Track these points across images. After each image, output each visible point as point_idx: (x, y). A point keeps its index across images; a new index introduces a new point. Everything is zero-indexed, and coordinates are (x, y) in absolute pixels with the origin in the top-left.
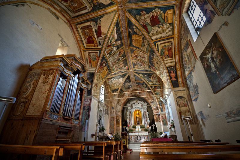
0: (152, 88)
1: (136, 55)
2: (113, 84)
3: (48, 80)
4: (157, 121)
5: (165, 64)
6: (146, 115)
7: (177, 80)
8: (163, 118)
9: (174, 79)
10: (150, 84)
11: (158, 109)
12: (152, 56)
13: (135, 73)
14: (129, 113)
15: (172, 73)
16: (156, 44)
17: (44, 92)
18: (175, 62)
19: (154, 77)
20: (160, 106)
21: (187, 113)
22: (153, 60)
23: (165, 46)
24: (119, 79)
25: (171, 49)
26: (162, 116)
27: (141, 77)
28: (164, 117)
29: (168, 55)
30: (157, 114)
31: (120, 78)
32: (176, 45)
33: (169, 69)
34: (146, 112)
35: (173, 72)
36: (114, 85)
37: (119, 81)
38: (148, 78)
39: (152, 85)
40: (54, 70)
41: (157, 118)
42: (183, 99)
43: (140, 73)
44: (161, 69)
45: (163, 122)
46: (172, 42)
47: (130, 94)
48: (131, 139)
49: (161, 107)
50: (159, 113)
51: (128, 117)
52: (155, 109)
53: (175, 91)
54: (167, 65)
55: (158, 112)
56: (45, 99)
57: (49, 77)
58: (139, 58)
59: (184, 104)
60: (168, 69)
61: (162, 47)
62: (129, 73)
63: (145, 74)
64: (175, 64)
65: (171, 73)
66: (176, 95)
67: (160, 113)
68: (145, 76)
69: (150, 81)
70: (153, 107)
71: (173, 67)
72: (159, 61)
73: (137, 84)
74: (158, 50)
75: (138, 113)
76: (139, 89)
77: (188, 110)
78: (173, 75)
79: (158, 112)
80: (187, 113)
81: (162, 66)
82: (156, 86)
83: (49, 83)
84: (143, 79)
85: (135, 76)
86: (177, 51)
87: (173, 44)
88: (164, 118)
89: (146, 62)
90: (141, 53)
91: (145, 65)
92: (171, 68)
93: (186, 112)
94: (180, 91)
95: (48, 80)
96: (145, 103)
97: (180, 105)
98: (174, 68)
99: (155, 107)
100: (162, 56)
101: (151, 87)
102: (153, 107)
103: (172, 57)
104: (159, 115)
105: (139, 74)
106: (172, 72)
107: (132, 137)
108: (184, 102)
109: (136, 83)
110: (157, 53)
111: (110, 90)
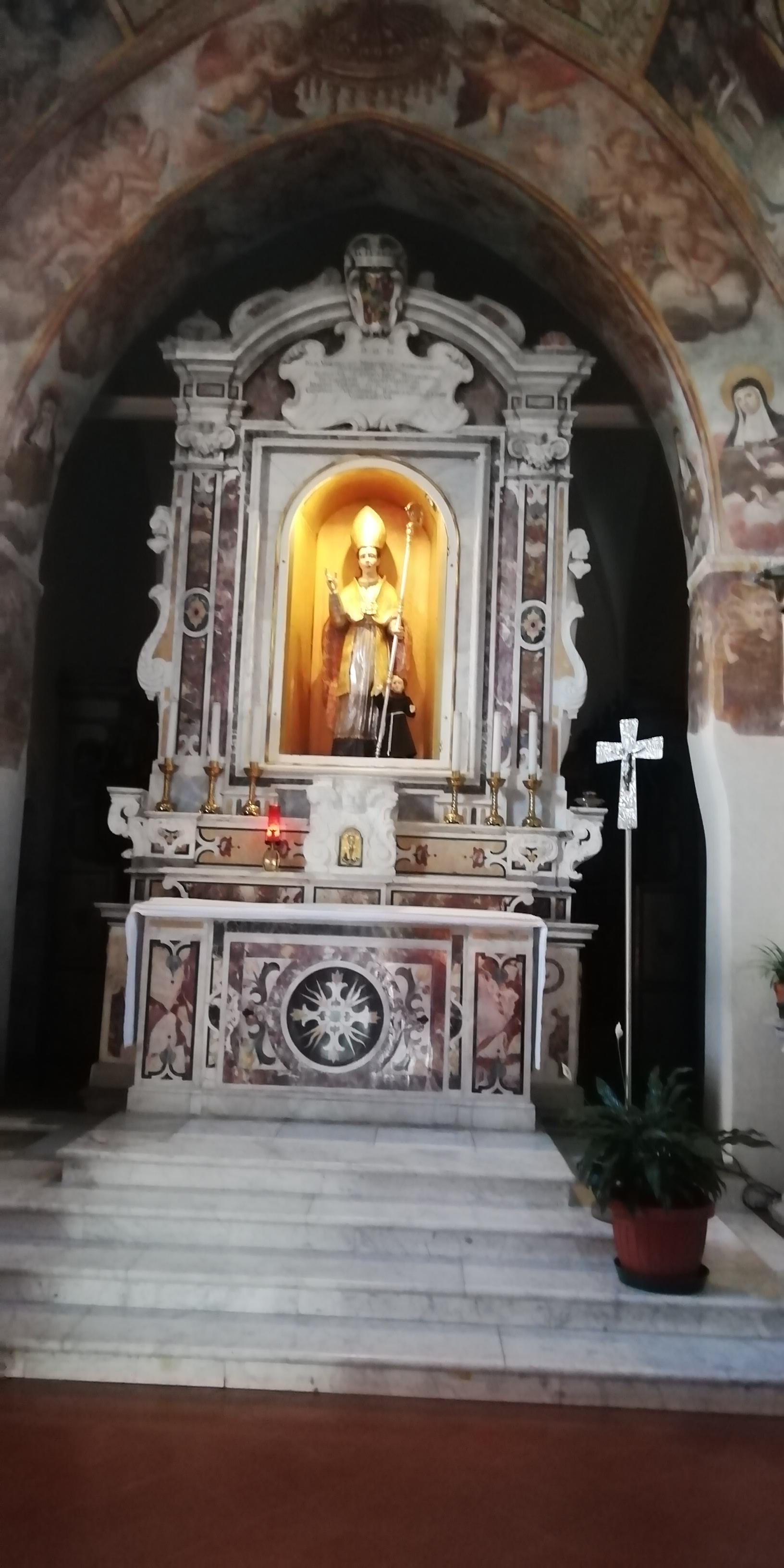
14: (198, 523)
34: (537, 534)
47: (241, 102)
48: (167, 1024)
51: (160, 594)
75: (382, 552)
96: (555, 342)
107: (188, 993)
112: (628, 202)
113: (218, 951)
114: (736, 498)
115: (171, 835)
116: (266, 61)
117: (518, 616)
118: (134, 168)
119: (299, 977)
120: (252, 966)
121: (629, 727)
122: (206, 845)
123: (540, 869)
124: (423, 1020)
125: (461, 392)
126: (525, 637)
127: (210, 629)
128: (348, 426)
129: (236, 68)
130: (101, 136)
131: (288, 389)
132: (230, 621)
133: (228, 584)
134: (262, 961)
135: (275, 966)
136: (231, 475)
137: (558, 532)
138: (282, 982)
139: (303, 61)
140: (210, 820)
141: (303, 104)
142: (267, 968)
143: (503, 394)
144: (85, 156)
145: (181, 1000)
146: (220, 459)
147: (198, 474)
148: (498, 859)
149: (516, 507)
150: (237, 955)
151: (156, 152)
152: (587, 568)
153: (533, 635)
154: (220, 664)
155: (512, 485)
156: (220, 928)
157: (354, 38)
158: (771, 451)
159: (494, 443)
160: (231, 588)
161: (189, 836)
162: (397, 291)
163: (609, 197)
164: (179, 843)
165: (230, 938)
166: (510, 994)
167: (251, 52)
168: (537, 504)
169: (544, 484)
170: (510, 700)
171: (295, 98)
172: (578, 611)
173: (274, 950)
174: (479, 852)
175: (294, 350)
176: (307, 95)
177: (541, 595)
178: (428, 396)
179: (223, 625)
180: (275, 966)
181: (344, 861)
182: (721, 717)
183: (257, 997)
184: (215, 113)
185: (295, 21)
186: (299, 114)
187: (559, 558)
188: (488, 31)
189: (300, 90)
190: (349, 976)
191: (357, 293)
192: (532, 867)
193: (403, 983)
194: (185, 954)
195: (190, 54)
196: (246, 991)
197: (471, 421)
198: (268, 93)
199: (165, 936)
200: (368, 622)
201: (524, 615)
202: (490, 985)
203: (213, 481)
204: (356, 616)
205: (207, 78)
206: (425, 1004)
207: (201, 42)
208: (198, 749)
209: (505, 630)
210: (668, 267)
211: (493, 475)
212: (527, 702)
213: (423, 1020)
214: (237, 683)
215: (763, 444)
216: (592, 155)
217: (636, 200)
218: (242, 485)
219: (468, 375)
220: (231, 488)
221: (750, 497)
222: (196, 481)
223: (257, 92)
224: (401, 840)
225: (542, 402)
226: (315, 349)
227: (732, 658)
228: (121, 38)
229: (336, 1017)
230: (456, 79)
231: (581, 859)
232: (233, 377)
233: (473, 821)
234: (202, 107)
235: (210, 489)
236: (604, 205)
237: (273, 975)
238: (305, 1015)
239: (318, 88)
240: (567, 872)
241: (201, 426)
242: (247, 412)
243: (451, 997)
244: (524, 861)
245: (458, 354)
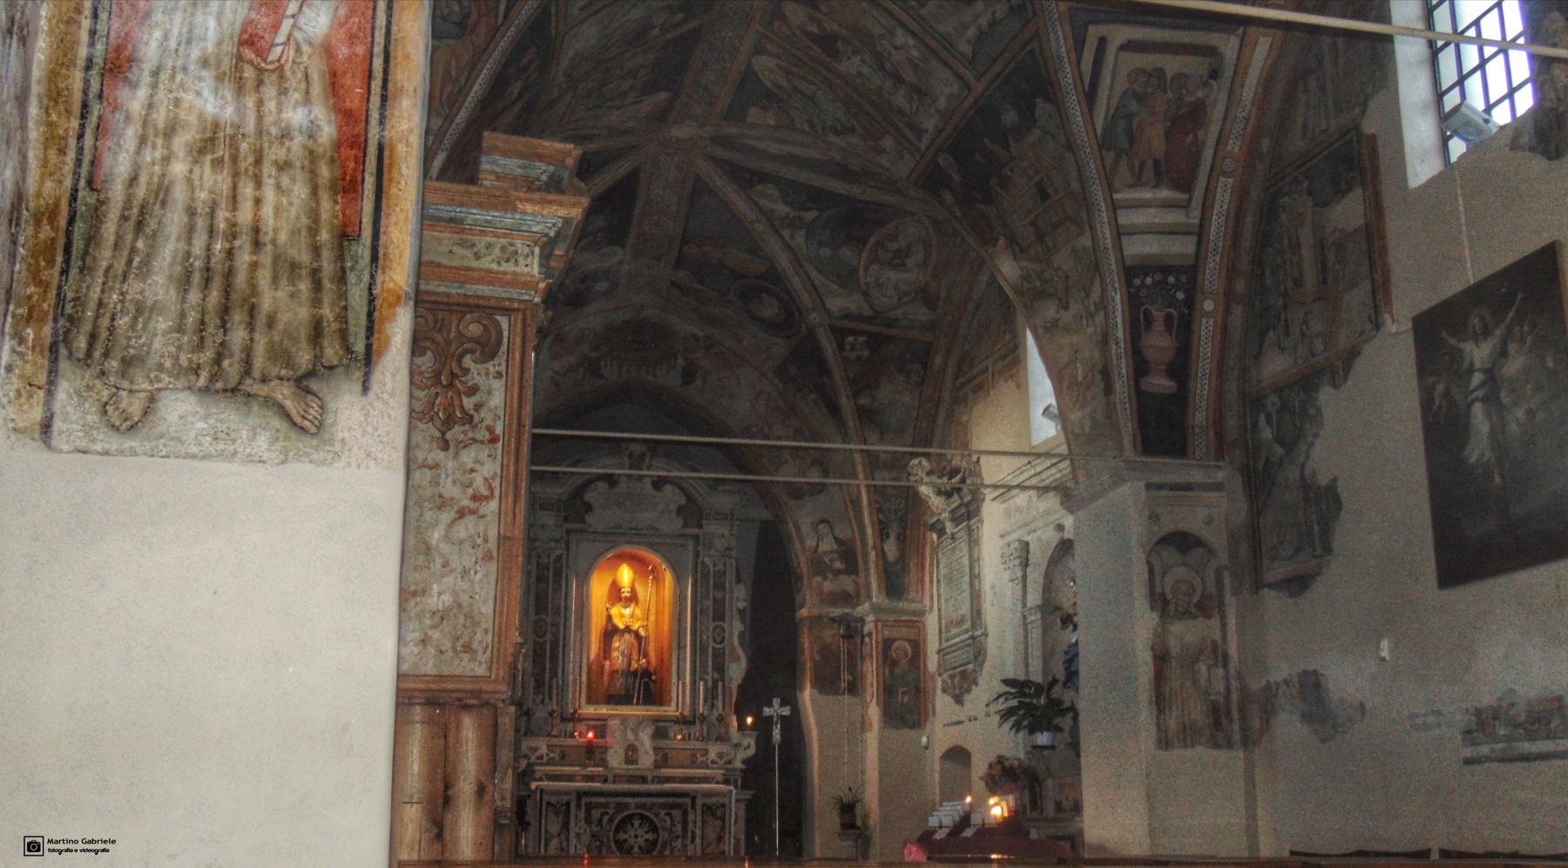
0: (841, 347)
1: (831, 26)
3: (468, 403)
4: (827, 683)
5: (1119, 233)
6: (719, 616)
7: (1181, 399)
8: (888, 660)
9: (1160, 383)
10: (836, 304)
11: (852, 568)
12: (1010, 117)
13: (716, 161)
15: (1159, 325)
16: (1094, 32)
17: (466, 502)
18: (1201, 233)
19: (894, 246)
20: (882, 535)
21: (1203, 668)
22: (1007, 147)
23: (1160, 73)
25: (1195, 115)
26: (888, 644)
27: (768, 215)
28: (901, 647)
29: (1156, 163)
30: (836, 612)
32: (1249, 91)
33: (1137, 282)
34: (720, 586)
35: (1168, 319)
39: (847, 316)
40: (504, 321)
41: (827, 654)
42: (1196, 555)
43: (765, 178)
44: (1062, 259)
45: (888, 692)
46: (1221, 56)
49: (891, 548)
50: (863, 609)
52: (819, 567)
53: (1149, 486)
54: (1138, 248)
55: (848, 598)
56: (488, 556)
57: (466, 371)
58: (852, 65)
59: (1195, 599)
60: (1129, 284)
61: (1135, 74)
63: (816, 197)
64: (1197, 255)
65: (1149, 323)
66: (1154, 517)
67: (877, 609)
68: (810, 216)
69: (847, 278)
70: (810, 543)
71: (1171, 279)
72: (1075, 186)
74: (1090, 97)
76: (686, 326)
77: (1214, 644)
78: (1159, 343)
79: (848, 598)
80: (1203, 668)
81: (1085, 241)
82: (890, 338)
83: (490, 429)
84: (773, 245)
85: (700, 189)
86: (1234, 146)
87: (1229, 73)
88: (904, 664)
89: (919, 132)
90: (901, 37)
91: (888, 142)
92: (1158, 277)
93: (1196, 661)
94: (1188, 487)
95: (468, 403)
97: (1166, 602)
98: (1177, 287)
99: (827, 545)
100: (1110, 157)
101: (839, 333)
102: (810, 543)
103: (1185, 185)
104: (852, 630)
105: (747, 178)
106: (1159, 315)
108: (1197, 582)
109: (680, 263)
110: (1077, 114)
112: (766, 427)
113: (579, 806)
114: (819, 579)
115: (536, 749)
117: (711, 630)
119: (619, 818)
120: (596, 814)
121: (776, 702)
122: (552, 755)
123: (726, 763)
124: (678, 837)
125: (680, 511)
126: (715, 641)
127: (548, 637)
128: (621, 528)
131: (589, 508)
132: (558, 632)
133: (557, 613)
134: (600, 811)
135: (607, 813)
136: (558, 552)
137: (731, 587)
138: (611, 821)
140: (555, 741)
141: (605, 372)
142: (602, 815)
143: (701, 510)
145: (561, 831)
146: (552, 543)
147: (540, 551)
148: (704, 759)
149: (709, 571)
150: (589, 808)
152: (745, 604)
153: (719, 639)
154: (554, 657)
155: (706, 559)
156: (581, 794)
158: (835, 555)
159: (696, 538)
160: (559, 616)
161: (543, 750)
162: (647, 460)
163: (757, 425)
164: (538, 754)
165: (584, 800)
166: (718, 822)
168: (719, 571)
169: (723, 561)
170: (707, 674)
172: (742, 628)
173: (606, 805)
174: (694, 756)
175: (593, 486)
177: (722, 618)
178: (662, 512)
179: (556, 635)
180: (607, 813)
181: (628, 761)
182: (812, 687)
183: (598, 829)
186: (600, 376)
187: (731, 598)
188: (696, 338)
189: (603, 363)
190: (643, 817)
191: (626, 459)
192: (721, 762)
193: (668, 820)
194: (563, 808)
196: (593, 826)
197: (685, 526)
198: (586, 365)
199: (554, 799)
200: (628, 629)
201: (714, 630)
202: (710, 819)
203: (549, 556)
204: (621, 626)
206: (678, 829)
208: (543, 702)
209: (705, 637)
210: (786, 462)
211: (697, 554)
212: (716, 676)
213: (678, 837)
214: (563, 669)
215: (831, 552)
216: (748, 404)
217: (770, 427)
218: (565, 556)
219: (683, 501)
220: (558, 559)
221: (825, 578)
222: (539, 557)
224: (656, 749)
225: (721, 517)
226: (602, 485)
227: (818, 657)
229: (636, 836)
230: (681, 362)
231: (746, 757)
232: (559, 500)
233: (690, 739)
235: (547, 561)
236: (754, 429)
237: (606, 818)
238: (622, 836)
240: (738, 764)
241: (543, 526)
242: (566, 520)
243: (691, 825)
244: (718, 760)
245: (677, 491)
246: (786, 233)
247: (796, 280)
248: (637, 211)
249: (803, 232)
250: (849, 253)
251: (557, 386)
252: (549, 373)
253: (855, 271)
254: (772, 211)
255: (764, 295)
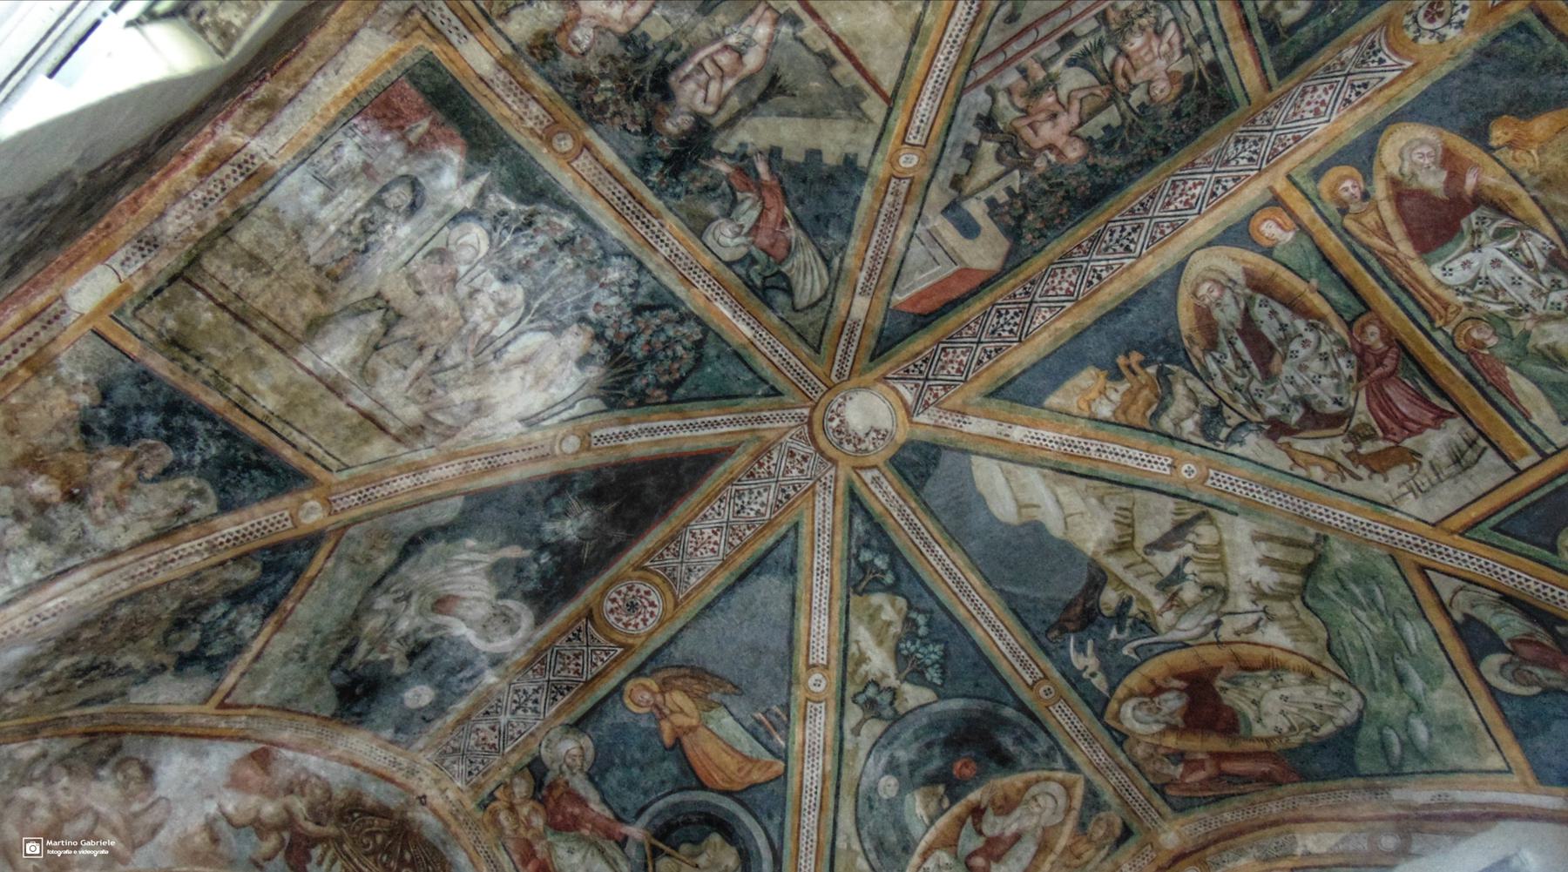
2: (331, 277)
19: (994, 825)
24: (541, 315)
27: (847, 658)
31: (575, 341)
36: (316, 326)
37: (487, 351)
38: (911, 776)
47: (259, 826)
62: (780, 424)
68: (914, 695)
73: (569, 750)
111: (113, 307)
116: (299, 805)
118: (116, 819)
129: (269, 793)
130: (102, 763)
139: (330, 829)
144: (70, 770)
151: (149, 819)
157: (379, 839)
167: (290, 791)
171: (309, 858)
176: (320, 864)
184: (229, 821)
185: (339, 794)
189: (316, 852)
195: (235, 751)
198: (286, 835)
205: (236, 783)
207: (249, 747)
223: (278, 828)
228: (206, 701)
234: (220, 806)
239: (333, 862)
246: (854, 714)
247: (810, 820)
248: (636, 552)
249: (876, 727)
250: (920, 811)
251: (215, 840)
252: (211, 808)
253: (907, 849)
254: (863, 659)
255: (716, 838)
